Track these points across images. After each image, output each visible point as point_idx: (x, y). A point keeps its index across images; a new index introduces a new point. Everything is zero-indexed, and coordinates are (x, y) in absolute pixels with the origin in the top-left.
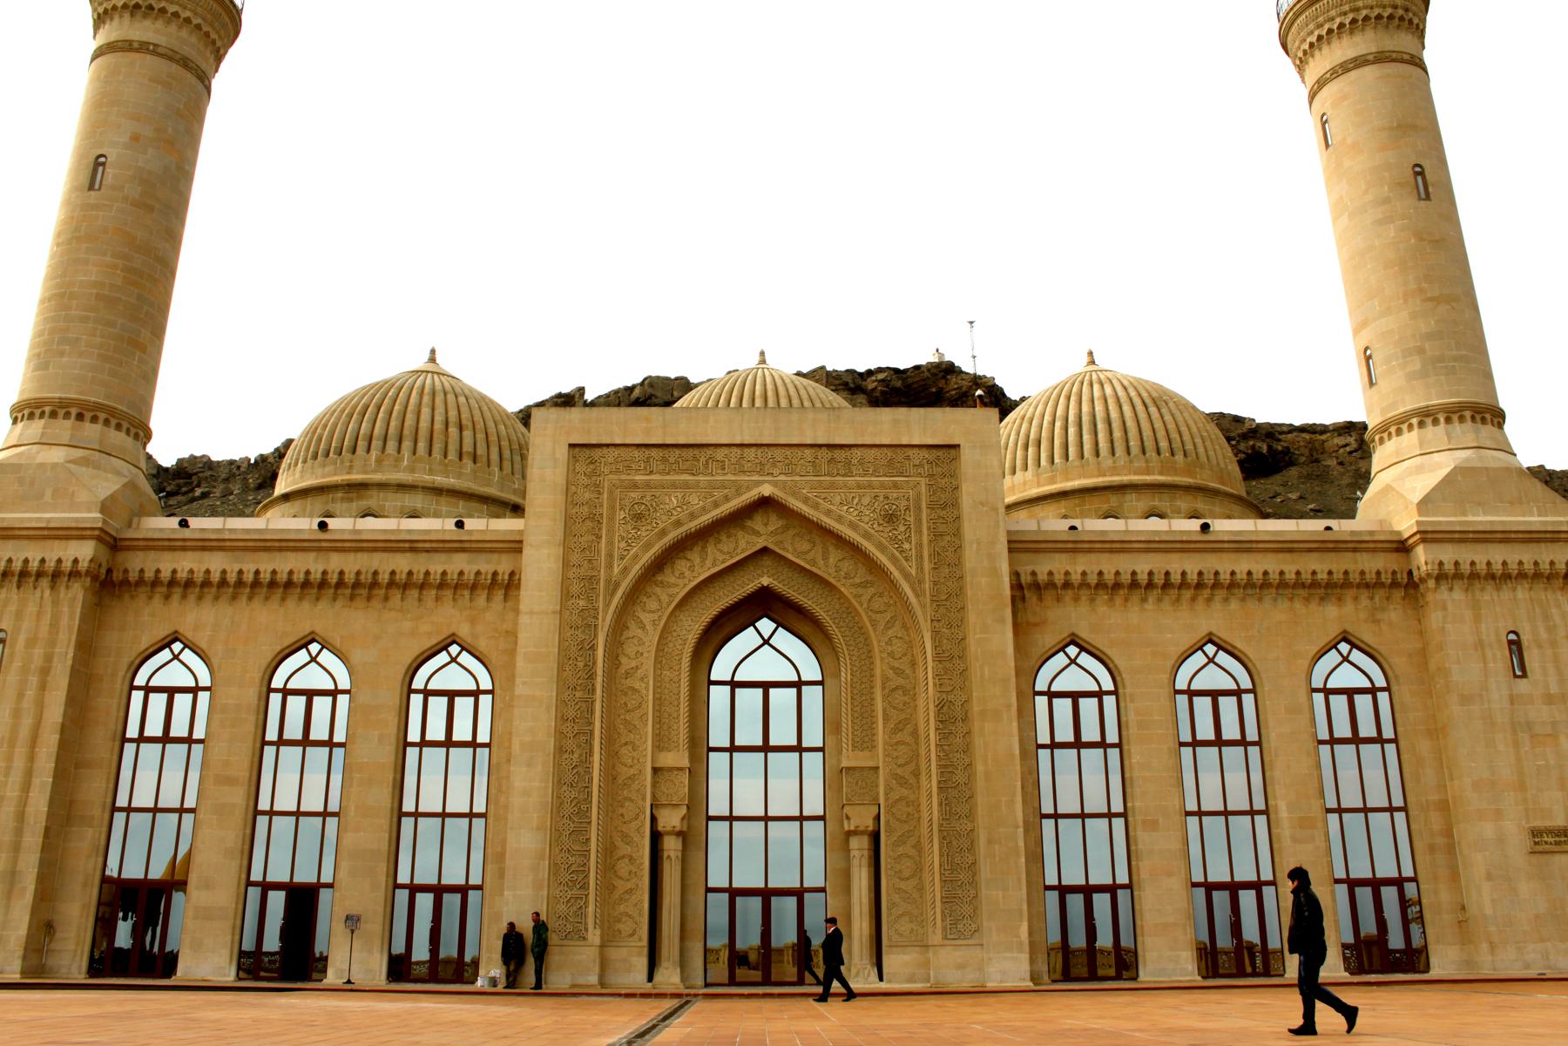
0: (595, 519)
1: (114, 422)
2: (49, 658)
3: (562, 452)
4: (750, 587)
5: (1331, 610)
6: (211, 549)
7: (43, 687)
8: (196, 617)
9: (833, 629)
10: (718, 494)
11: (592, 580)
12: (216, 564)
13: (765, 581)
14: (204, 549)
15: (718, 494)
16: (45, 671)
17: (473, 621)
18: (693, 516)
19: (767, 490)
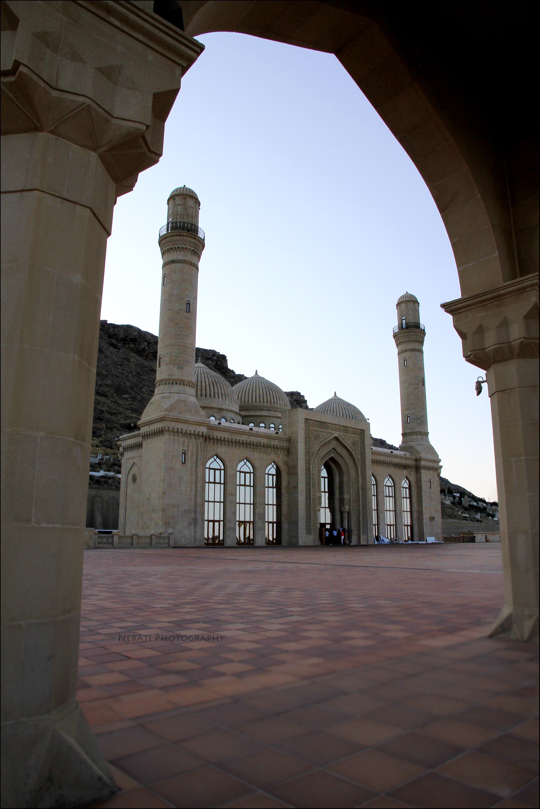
0: (309, 437)
1: (174, 382)
2: (197, 459)
3: (304, 420)
4: (330, 457)
5: (405, 471)
6: (226, 431)
7: (196, 467)
8: (222, 450)
9: (344, 468)
10: (329, 435)
11: (309, 452)
12: (226, 435)
13: (332, 455)
14: (224, 431)
15: (329, 435)
16: (197, 463)
17: (278, 457)
18: (326, 439)
19: (336, 435)
